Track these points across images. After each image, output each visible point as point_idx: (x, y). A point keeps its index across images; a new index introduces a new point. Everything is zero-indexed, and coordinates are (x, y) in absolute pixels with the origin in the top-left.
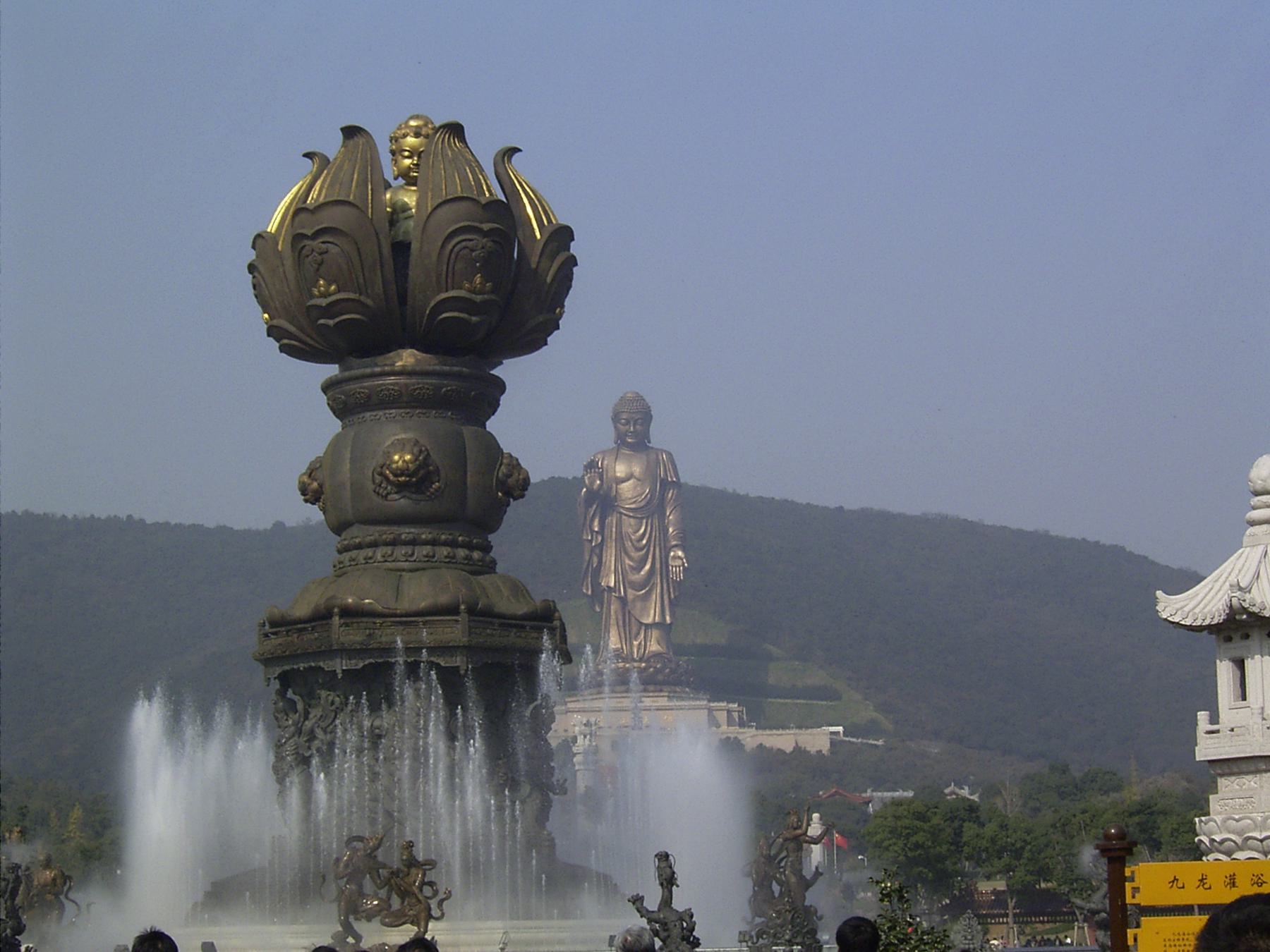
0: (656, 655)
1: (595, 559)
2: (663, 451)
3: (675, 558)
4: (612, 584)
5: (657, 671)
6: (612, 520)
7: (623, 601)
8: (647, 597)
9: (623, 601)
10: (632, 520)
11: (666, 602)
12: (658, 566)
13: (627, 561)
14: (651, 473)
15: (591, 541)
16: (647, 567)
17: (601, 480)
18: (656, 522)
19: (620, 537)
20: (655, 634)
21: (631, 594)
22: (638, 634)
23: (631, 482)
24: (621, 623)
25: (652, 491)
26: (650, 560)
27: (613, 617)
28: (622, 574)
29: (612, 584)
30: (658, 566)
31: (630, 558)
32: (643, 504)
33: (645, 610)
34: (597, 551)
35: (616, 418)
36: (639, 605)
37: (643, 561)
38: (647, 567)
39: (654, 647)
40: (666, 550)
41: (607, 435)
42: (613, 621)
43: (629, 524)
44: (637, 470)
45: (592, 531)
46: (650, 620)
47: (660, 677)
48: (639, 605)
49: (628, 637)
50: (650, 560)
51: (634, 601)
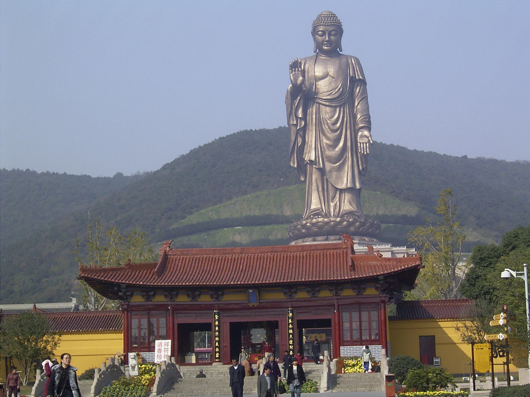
0: (350, 213)
1: (300, 140)
2: (351, 57)
3: (362, 136)
4: (313, 158)
5: (350, 224)
6: (313, 109)
7: (322, 171)
8: (340, 168)
9: (322, 171)
11: (356, 172)
12: (349, 144)
13: (325, 141)
14: (343, 71)
15: (296, 125)
16: (341, 144)
17: (304, 76)
19: (319, 123)
20: (347, 197)
21: (328, 166)
22: (334, 197)
23: (327, 79)
25: (344, 86)
26: (343, 137)
27: (314, 184)
28: (320, 149)
29: (313, 158)
30: (349, 144)
31: (328, 138)
32: (336, 95)
33: (339, 178)
34: (301, 133)
35: (314, 32)
36: (334, 174)
37: (338, 140)
38: (341, 144)
39: (347, 207)
40: (355, 132)
41: (308, 47)
42: (314, 187)
43: (326, 112)
44: (332, 71)
45: (297, 118)
46: (343, 186)
47: (352, 229)
48: (334, 174)
49: (326, 199)
50: (343, 137)
51: (330, 171)
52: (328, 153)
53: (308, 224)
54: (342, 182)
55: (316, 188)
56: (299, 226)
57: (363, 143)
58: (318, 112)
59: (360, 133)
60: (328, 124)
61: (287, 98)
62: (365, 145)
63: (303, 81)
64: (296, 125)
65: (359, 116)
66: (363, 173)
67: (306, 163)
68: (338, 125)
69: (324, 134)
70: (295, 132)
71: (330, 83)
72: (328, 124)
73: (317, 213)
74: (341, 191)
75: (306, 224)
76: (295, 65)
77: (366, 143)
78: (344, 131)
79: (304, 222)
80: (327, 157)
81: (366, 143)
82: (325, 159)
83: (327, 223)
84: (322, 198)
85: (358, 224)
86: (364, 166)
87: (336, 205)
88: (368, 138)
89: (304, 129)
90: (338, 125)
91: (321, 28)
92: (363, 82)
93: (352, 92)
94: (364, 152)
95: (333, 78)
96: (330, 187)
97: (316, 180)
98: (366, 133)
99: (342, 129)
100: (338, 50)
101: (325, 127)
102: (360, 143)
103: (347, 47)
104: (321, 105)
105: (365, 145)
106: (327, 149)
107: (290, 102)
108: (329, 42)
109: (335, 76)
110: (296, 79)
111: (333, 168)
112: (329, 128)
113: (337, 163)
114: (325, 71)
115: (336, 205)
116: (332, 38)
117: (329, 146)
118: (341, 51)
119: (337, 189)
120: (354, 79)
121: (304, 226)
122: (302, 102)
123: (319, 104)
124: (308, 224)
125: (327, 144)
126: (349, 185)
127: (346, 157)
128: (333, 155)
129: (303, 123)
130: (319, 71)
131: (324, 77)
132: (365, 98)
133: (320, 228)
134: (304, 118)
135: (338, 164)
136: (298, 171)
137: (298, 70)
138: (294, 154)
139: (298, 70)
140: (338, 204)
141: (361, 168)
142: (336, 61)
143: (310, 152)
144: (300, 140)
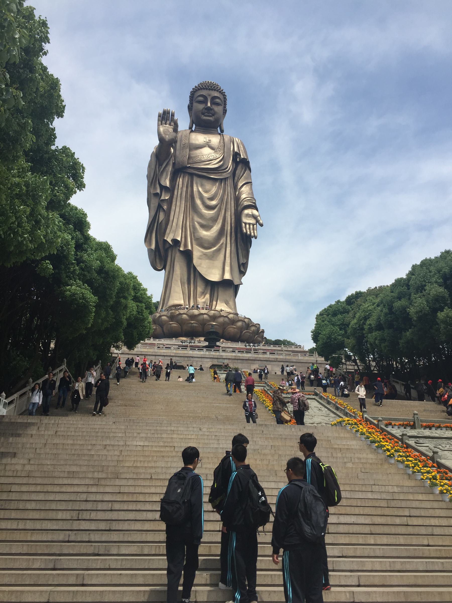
9: (188, 256)
12: (228, 228)
13: (196, 219)
21: (197, 252)
24: (186, 277)
37: (214, 220)
53: (164, 318)
57: (250, 224)
61: (149, 166)
62: (251, 226)
66: (242, 269)
67: (167, 246)
70: (157, 204)
75: (160, 316)
78: (223, 211)
79: (158, 315)
81: (253, 225)
85: (240, 324)
90: (214, 203)
91: (204, 93)
94: (250, 232)
99: (220, 209)
100: (219, 129)
101: (198, 202)
104: (195, 178)
105: (251, 226)
107: (153, 167)
112: (204, 203)
113: (210, 248)
120: (238, 156)
122: (170, 168)
134: (171, 190)
136: (155, 257)
143: (175, 232)
144: (162, 216)
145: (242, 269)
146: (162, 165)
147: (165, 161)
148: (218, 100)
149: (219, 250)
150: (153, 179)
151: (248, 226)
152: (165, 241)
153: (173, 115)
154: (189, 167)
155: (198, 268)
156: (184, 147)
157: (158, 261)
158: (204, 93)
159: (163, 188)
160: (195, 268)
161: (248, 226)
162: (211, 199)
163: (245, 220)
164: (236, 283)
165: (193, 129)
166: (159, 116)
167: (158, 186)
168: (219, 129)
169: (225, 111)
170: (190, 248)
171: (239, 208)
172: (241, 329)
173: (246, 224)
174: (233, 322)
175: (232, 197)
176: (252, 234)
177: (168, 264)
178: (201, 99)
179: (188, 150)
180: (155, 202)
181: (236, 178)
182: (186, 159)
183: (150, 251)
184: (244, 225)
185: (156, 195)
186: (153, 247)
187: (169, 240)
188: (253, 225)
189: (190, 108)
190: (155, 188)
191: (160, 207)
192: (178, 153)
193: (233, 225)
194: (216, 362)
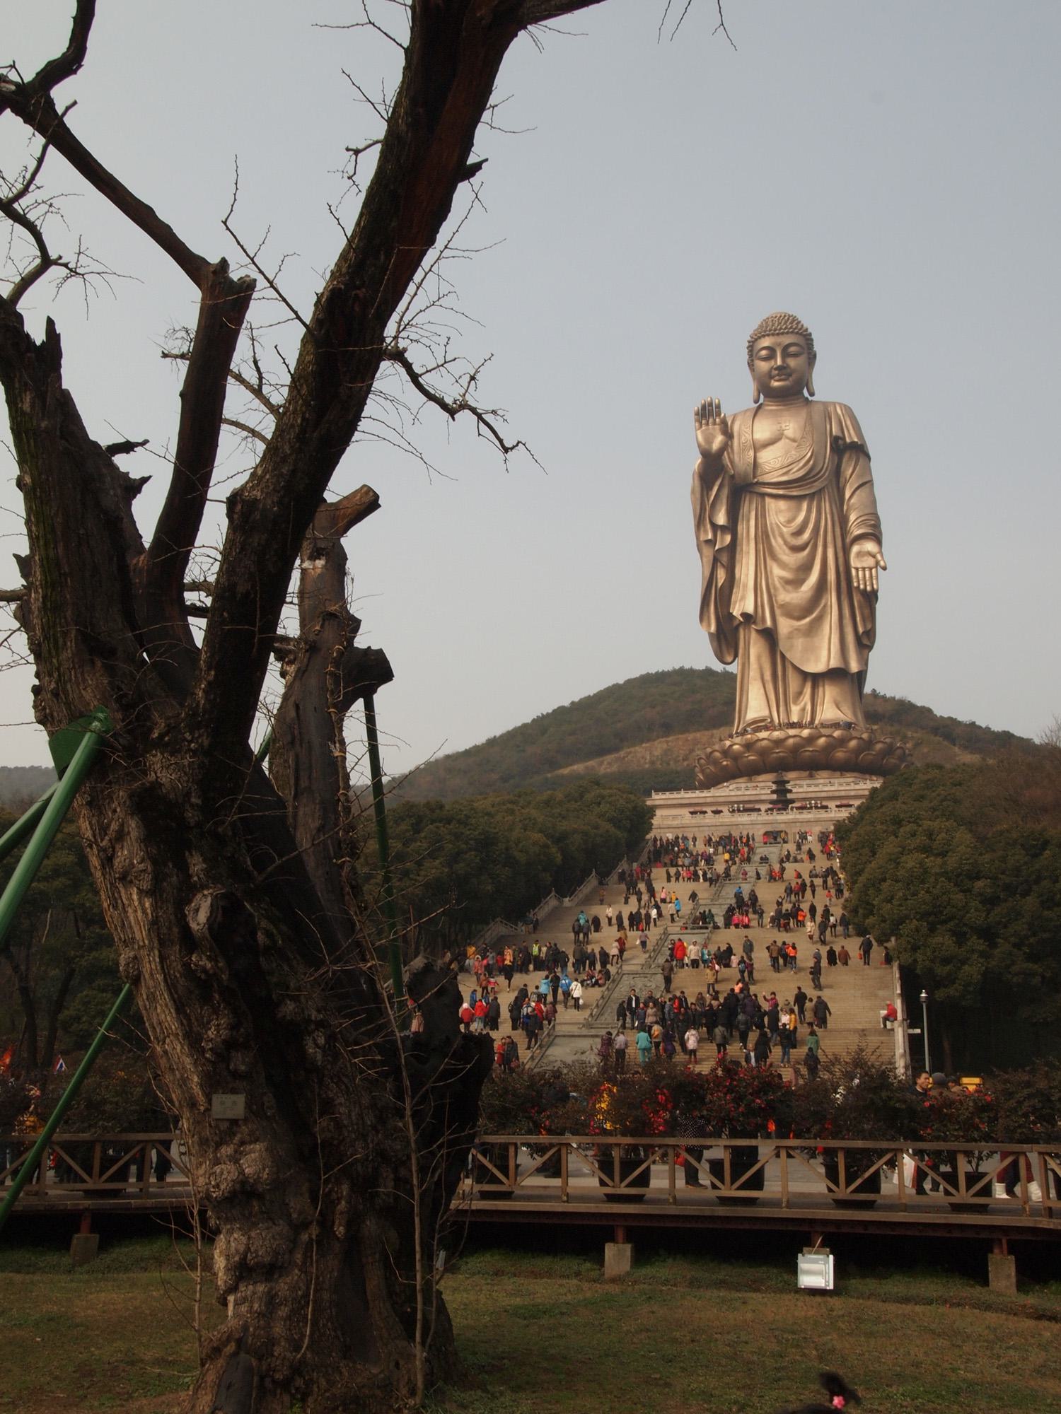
1: (721, 575)
2: (834, 404)
3: (859, 554)
4: (750, 609)
7: (770, 636)
8: (812, 630)
9: (770, 636)
10: (782, 504)
11: (850, 638)
12: (832, 576)
13: (777, 572)
18: (826, 506)
19: (763, 537)
22: (800, 693)
24: (768, 676)
30: (832, 576)
31: (783, 565)
33: (811, 650)
34: (724, 558)
36: (799, 642)
37: (806, 568)
46: (817, 665)
47: (840, 755)
49: (782, 698)
51: (790, 636)
52: (785, 596)
53: (736, 747)
54: (817, 660)
55: (758, 676)
56: (717, 754)
57: (864, 569)
58: (762, 515)
59: (855, 549)
60: (782, 536)
61: (693, 492)
62: (867, 573)
63: (725, 447)
64: (711, 543)
65: (852, 517)
66: (865, 641)
67: (736, 623)
68: (806, 535)
69: (774, 557)
70: (711, 558)
71: (787, 452)
72: (782, 536)
73: (759, 725)
74: (816, 679)
76: (707, 413)
77: (871, 569)
78: (820, 549)
80: (782, 606)
82: (778, 612)
83: (778, 742)
84: (772, 697)
85: (853, 743)
86: (869, 627)
87: (803, 709)
88: (874, 556)
89: (732, 549)
90: (806, 535)
91: (766, 342)
92: (860, 450)
93: (837, 472)
95: (794, 440)
96: (790, 671)
97: (759, 658)
98: (870, 546)
100: (805, 392)
101: (777, 543)
102: (857, 569)
103: (827, 383)
104: (768, 500)
105: (867, 573)
106: (781, 590)
107: (698, 495)
108: (783, 371)
109: (798, 436)
110: (709, 440)
111: (797, 629)
112: (786, 542)
113: (804, 617)
114: (775, 427)
115: (803, 709)
116: (792, 362)
117: (788, 582)
118: (812, 394)
119: (805, 676)
121: (726, 753)
122: (725, 492)
123: (763, 495)
124: (736, 747)
125: (781, 578)
126: (834, 663)
127: (825, 606)
128: (795, 601)
129: (728, 538)
130: (763, 430)
131: (775, 443)
132: (867, 484)
133: (763, 753)
134: (732, 527)
135: (808, 620)
137: (714, 423)
138: (708, 605)
139: (714, 423)
140: (809, 707)
141: (861, 630)
142: (804, 413)
143: (743, 598)
144: (721, 575)
145: (865, 641)
146: (711, 489)
147: (716, 479)
148: (792, 349)
149: (820, 618)
150: (702, 517)
151: (860, 573)
152: (731, 617)
153: (718, 407)
154: (757, 483)
155: (788, 655)
156: (743, 449)
157: (724, 647)
158: (766, 342)
159: (715, 527)
160: (783, 657)
161: (860, 573)
162: (799, 532)
163: (854, 562)
164: (854, 667)
165: (761, 400)
166: (697, 414)
167: (709, 526)
168: (805, 392)
169: (812, 358)
170: (769, 623)
171: (848, 540)
172: (858, 751)
173: (857, 569)
174: (842, 742)
175: (836, 518)
176: (869, 588)
177: (741, 651)
178: (764, 353)
179: (752, 453)
180: (709, 553)
181: (842, 480)
182: (750, 470)
183: (711, 635)
184: (854, 572)
185: (708, 542)
186: (713, 629)
187: (736, 611)
188: (871, 569)
189: (751, 365)
190: (706, 531)
191: (716, 561)
192: (736, 459)
193: (841, 569)
194: (769, 828)
